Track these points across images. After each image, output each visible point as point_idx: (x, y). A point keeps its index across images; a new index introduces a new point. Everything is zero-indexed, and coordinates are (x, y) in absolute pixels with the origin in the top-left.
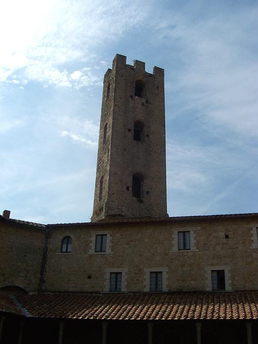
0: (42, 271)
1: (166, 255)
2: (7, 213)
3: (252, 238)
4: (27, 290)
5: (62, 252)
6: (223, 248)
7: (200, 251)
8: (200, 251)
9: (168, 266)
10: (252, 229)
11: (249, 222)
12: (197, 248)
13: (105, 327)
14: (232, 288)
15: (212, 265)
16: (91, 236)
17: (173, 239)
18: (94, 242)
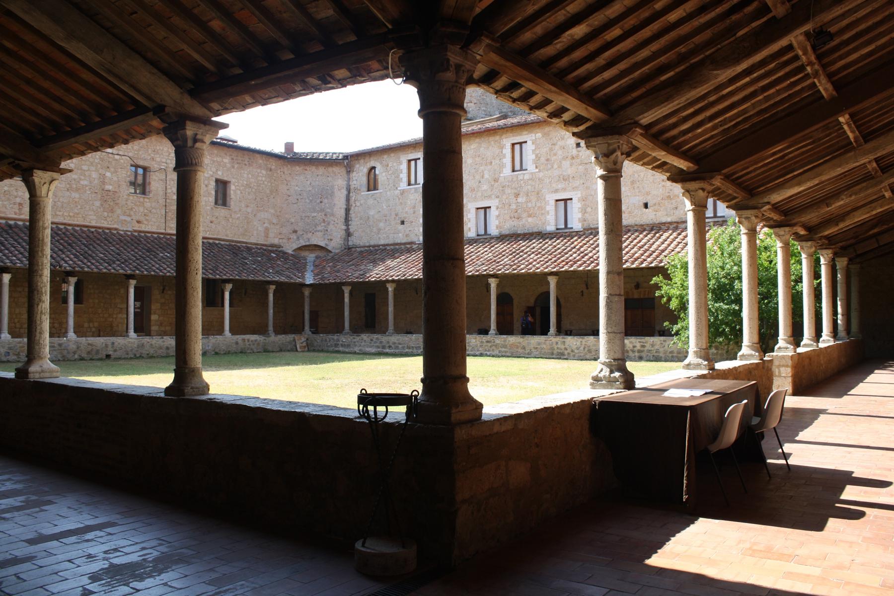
0: (347, 220)
1: (496, 180)
2: (289, 146)
4: (329, 248)
5: (368, 190)
6: (571, 165)
7: (540, 171)
8: (540, 171)
9: (497, 197)
12: (536, 167)
13: (390, 289)
14: (583, 225)
15: (556, 191)
16: (401, 163)
17: (504, 156)
18: (405, 171)
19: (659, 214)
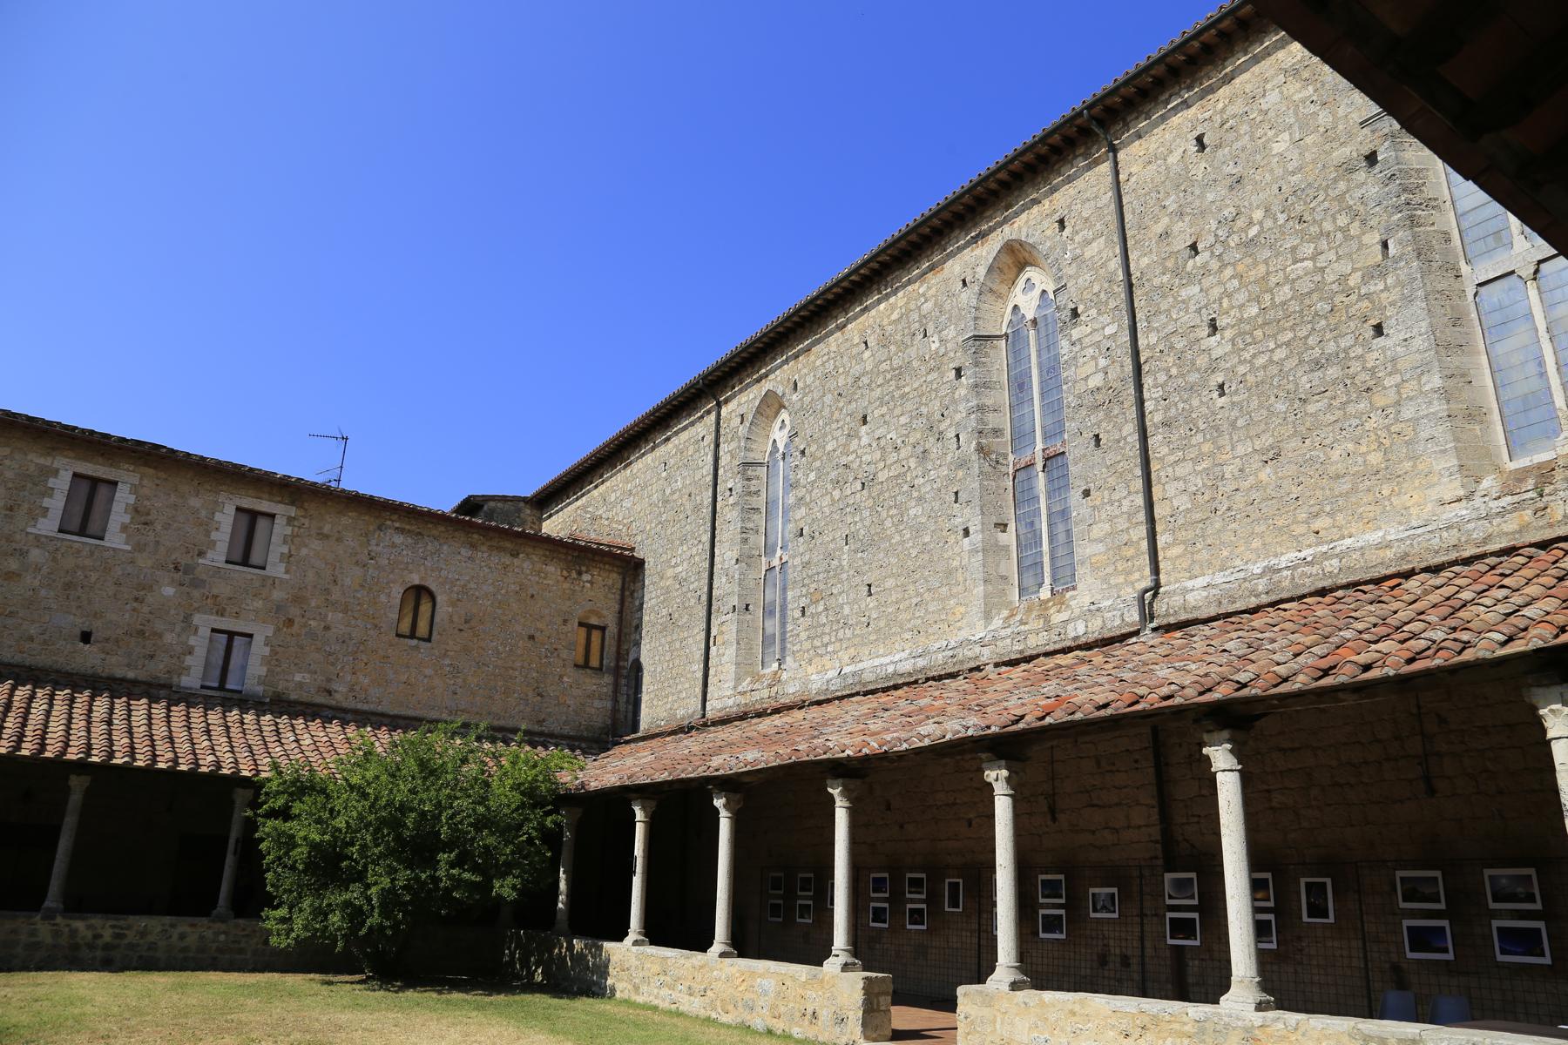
3: (46, 502)
10: (56, 473)
11: (53, 449)
19: (114, 659)
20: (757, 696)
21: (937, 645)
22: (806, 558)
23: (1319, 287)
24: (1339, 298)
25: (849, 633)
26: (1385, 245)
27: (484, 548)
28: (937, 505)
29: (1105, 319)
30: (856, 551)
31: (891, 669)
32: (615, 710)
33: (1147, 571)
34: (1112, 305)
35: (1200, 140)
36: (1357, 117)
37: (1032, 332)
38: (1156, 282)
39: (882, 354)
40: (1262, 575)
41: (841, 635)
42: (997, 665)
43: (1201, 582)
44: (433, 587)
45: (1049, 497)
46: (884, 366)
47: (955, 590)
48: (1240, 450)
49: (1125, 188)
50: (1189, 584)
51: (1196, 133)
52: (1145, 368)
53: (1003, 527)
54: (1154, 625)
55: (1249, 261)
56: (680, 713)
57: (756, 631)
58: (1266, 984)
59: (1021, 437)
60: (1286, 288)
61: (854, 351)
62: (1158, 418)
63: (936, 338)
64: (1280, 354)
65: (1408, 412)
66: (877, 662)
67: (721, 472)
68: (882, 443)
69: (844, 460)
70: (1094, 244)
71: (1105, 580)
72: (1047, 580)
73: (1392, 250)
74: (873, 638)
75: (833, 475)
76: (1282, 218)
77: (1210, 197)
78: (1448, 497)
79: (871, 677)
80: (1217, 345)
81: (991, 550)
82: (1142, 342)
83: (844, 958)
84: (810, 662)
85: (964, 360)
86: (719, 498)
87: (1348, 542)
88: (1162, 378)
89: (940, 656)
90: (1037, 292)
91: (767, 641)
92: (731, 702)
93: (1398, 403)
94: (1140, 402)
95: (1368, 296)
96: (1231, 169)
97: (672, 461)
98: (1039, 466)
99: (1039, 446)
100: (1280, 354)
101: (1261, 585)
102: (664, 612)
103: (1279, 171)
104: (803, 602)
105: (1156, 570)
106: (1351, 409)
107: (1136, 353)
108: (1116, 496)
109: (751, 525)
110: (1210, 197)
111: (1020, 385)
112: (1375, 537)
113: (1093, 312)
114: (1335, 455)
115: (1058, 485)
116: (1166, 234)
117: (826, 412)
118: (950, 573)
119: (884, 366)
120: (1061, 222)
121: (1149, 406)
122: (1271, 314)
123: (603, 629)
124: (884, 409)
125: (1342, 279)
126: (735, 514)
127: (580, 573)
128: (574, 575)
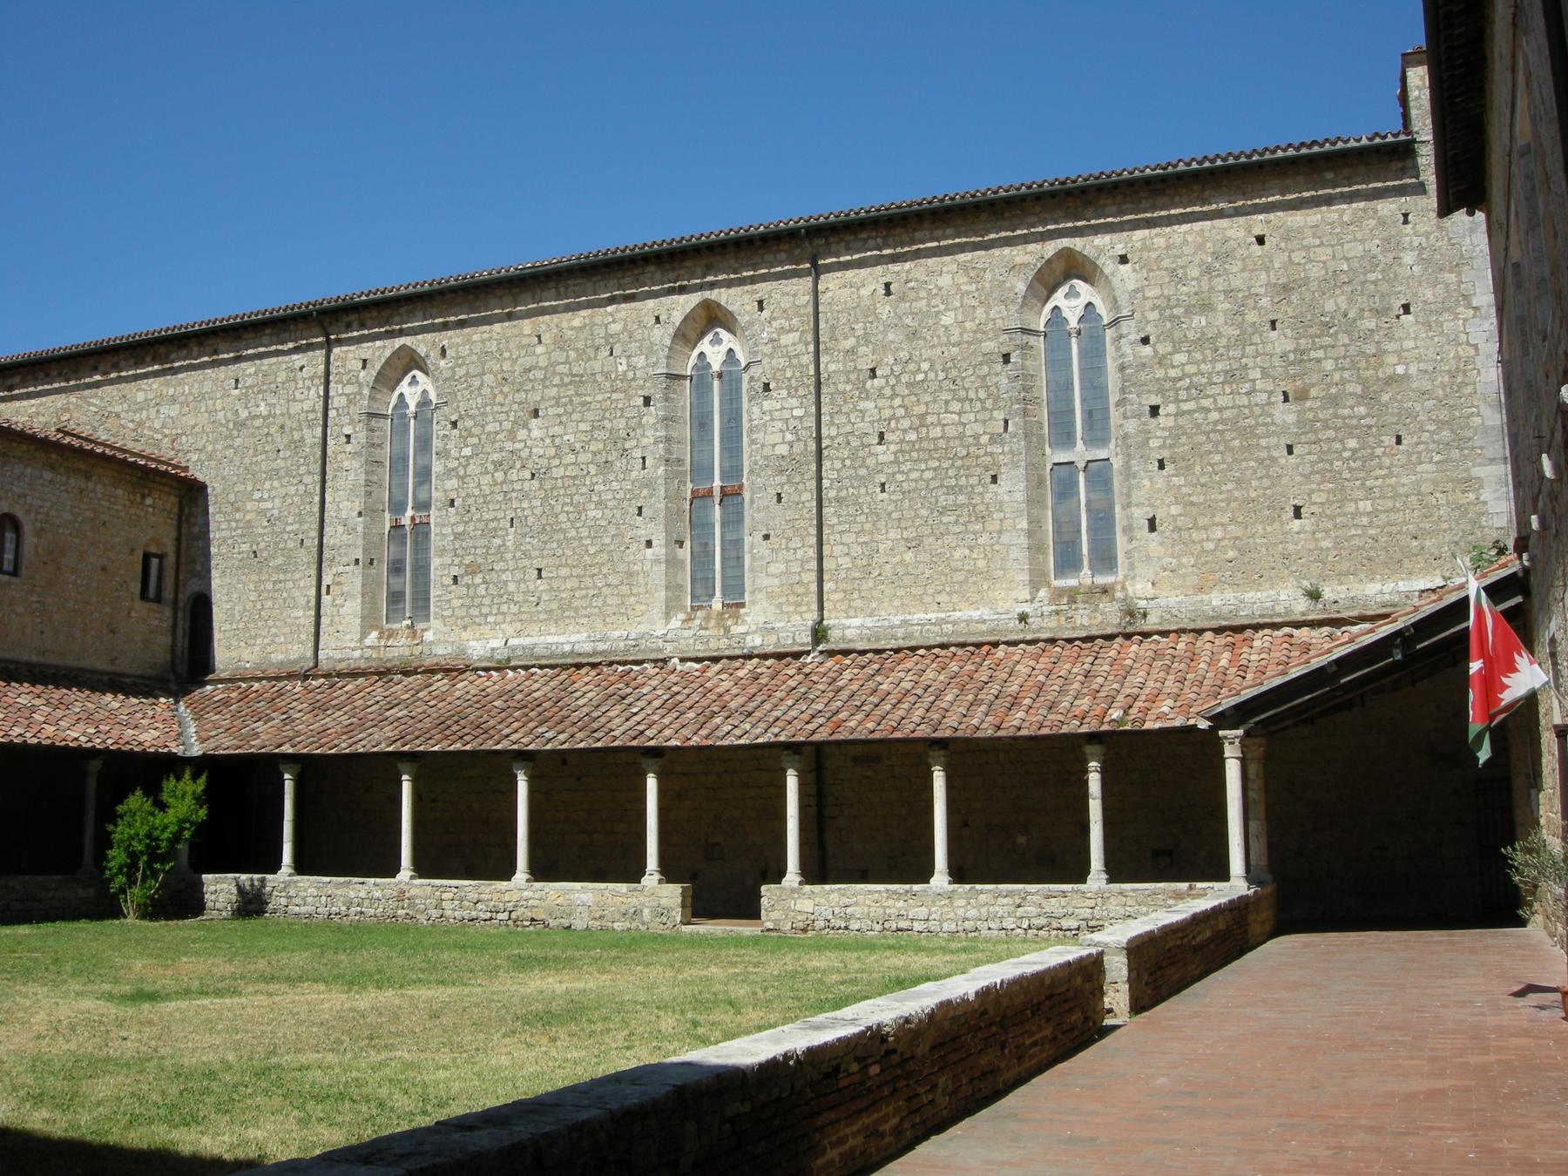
20: (395, 653)
21: (617, 634)
22: (460, 529)
23: (961, 436)
24: (972, 449)
25: (514, 609)
26: (1006, 422)
27: (62, 470)
28: (618, 514)
29: (794, 402)
30: (524, 535)
31: (567, 648)
32: (173, 647)
33: (815, 606)
34: (801, 392)
35: (887, 285)
36: (1000, 323)
37: (716, 383)
38: (841, 387)
39: (559, 356)
40: (900, 626)
41: (504, 608)
42: (683, 660)
43: (857, 622)
44: (20, 513)
45: (723, 525)
46: (560, 369)
47: (635, 590)
48: (892, 535)
49: (823, 299)
50: (847, 622)
51: (886, 280)
52: (825, 453)
53: (681, 543)
54: (820, 648)
55: (913, 398)
56: (278, 657)
57: (380, 585)
58: (950, 874)
59: (701, 470)
60: (939, 429)
61: (525, 341)
62: (832, 494)
63: (624, 361)
64: (928, 475)
65: (1005, 539)
66: (550, 639)
67: (332, 413)
68: (558, 441)
69: (509, 446)
70: (791, 336)
71: (779, 606)
72: (718, 593)
73: (1010, 428)
74: (543, 616)
75: (496, 457)
76: (942, 376)
77: (891, 336)
78: (1021, 598)
79: (545, 652)
80: (884, 453)
81: (672, 563)
82: (824, 432)
83: (657, 876)
84: (465, 628)
85: (657, 396)
86: (330, 442)
87: (958, 614)
88: (838, 465)
89: (622, 644)
90: (724, 348)
91: (395, 598)
92: (357, 653)
93: (1000, 532)
94: (819, 479)
95: (992, 454)
96: (908, 321)
97: (250, 382)
98: (717, 500)
99: (717, 483)
100: (928, 475)
101: (901, 632)
102: (245, 547)
103: (944, 340)
104: (455, 571)
105: (821, 608)
106: (971, 527)
107: (819, 439)
108: (791, 545)
109: (375, 478)
110: (891, 336)
111: (701, 423)
112: (975, 614)
113: (784, 393)
114: (957, 555)
115: (734, 520)
116: (851, 352)
117: (486, 391)
118: (630, 574)
119: (560, 369)
120: (760, 303)
121: (826, 483)
122: (925, 444)
123: (161, 557)
124: (561, 410)
125: (976, 437)
126: (356, 464)
127: (144, 497)
128: (138, 499)
